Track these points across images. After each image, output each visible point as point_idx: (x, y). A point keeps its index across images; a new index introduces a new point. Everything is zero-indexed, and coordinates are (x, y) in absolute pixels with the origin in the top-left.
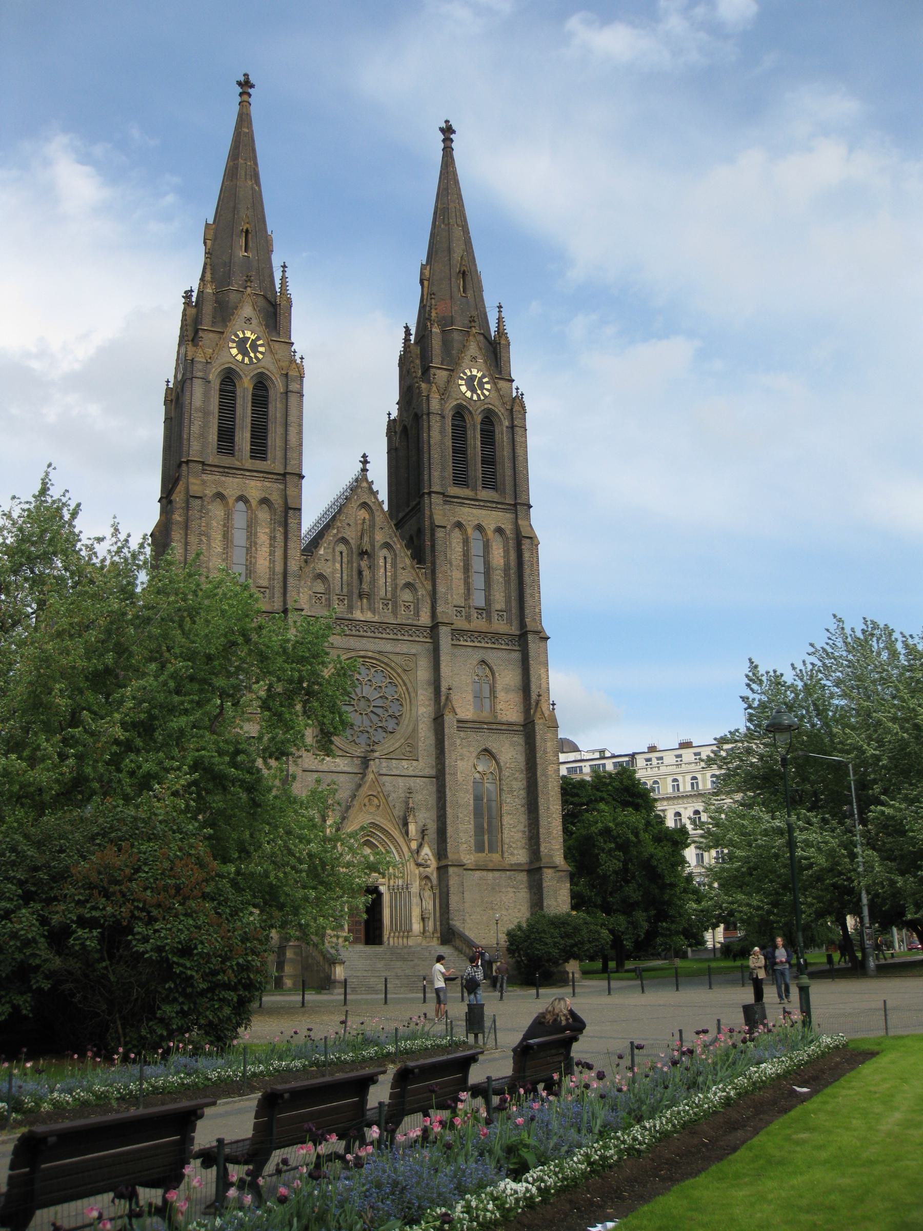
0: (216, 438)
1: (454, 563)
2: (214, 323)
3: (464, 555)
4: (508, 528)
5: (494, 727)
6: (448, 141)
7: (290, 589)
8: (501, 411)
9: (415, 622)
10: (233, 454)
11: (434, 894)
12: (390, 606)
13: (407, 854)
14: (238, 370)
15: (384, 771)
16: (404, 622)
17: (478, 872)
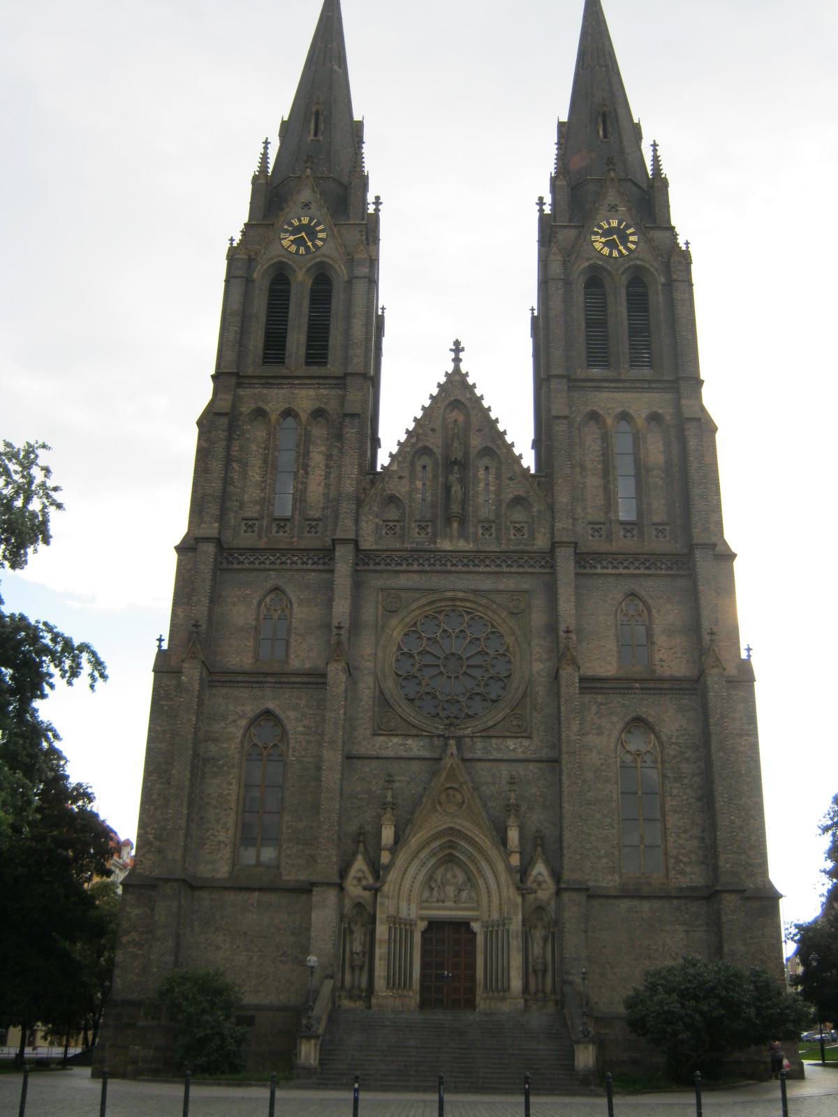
0: (261, 345)
2: (265, 217)
3: (604, 455)
4: (667, 412)
5: (651, 685)
7: (342, 516)
9: (529, 548)
10: (283, 363)
11: (553, 934)
12: (493, 530)
13: (504, 877)
14: (290, 263)
15: (479, 754)
16: (511, 548)
17: (625, 901)
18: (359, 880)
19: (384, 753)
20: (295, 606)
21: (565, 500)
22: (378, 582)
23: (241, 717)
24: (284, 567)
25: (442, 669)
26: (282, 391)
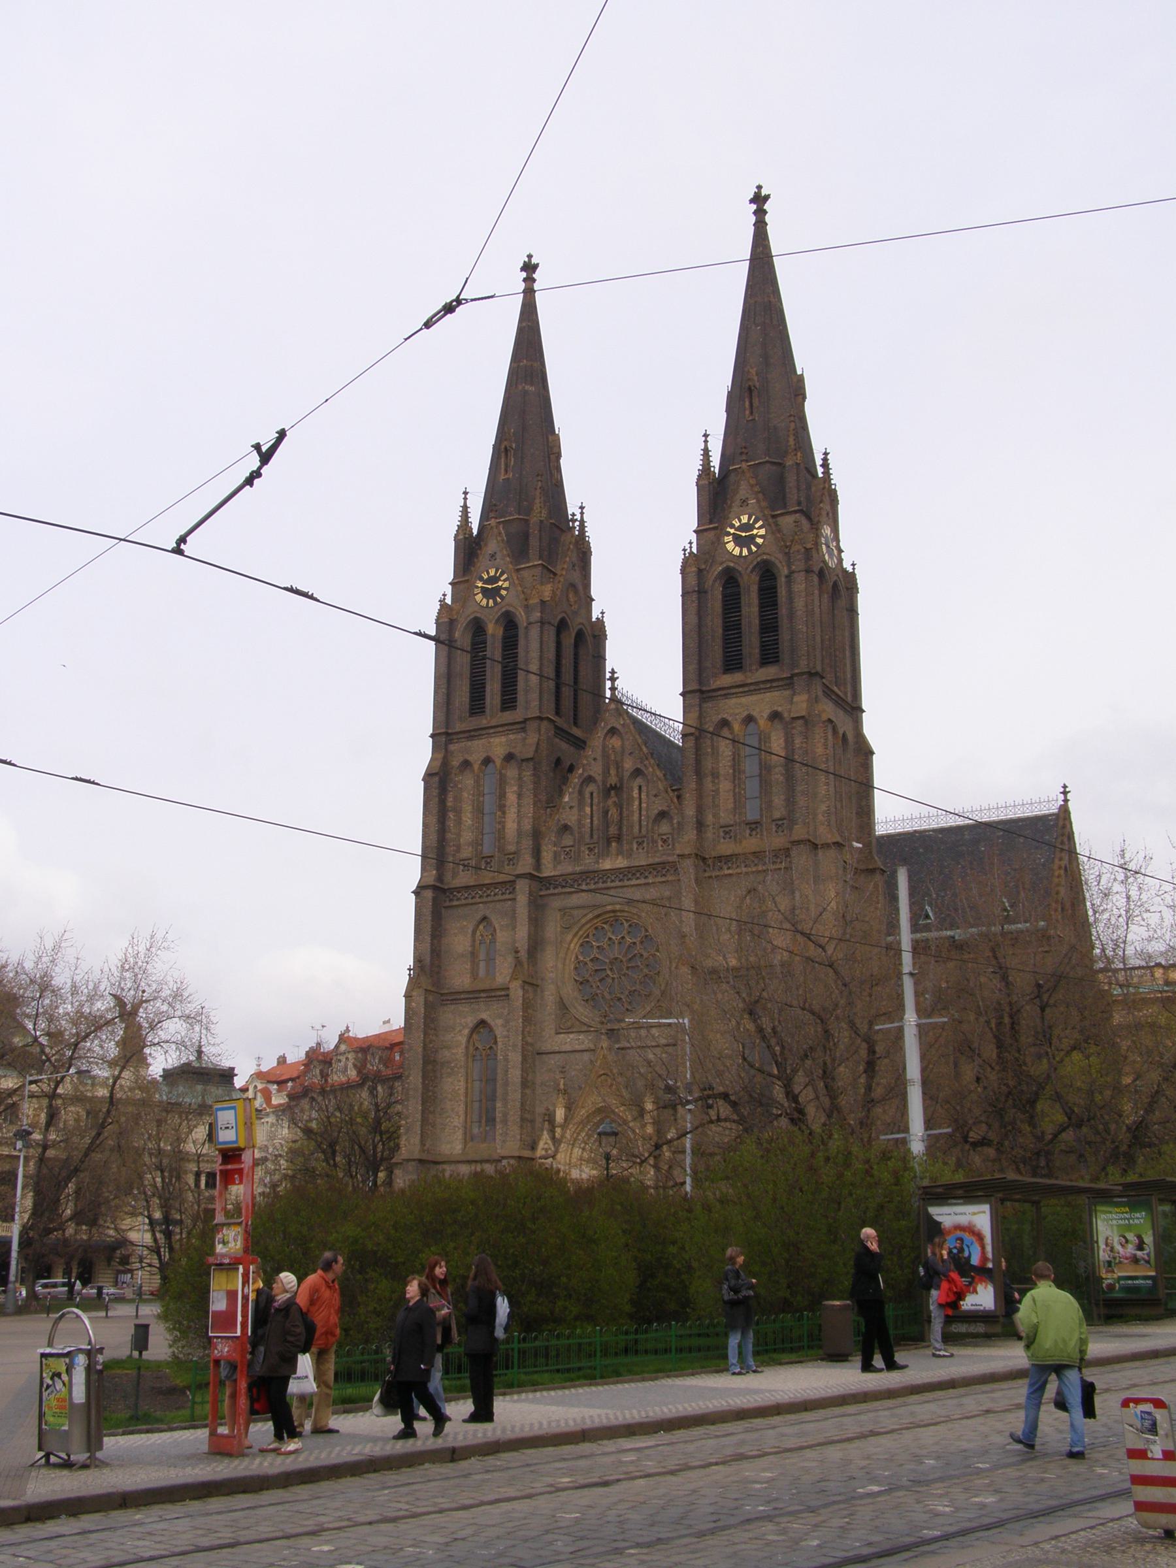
1: (722, 772)
2: (464, 574)
6: (760, 213)
8: (777, 559)
18: (546, 1150)
19: (564, 1048)
20: (498, 931)
21: (691, 813)
22: (556, 903)
23: (464, 1027)
24: (489, 899)
25: (609, 972)
26: (480, 742)
